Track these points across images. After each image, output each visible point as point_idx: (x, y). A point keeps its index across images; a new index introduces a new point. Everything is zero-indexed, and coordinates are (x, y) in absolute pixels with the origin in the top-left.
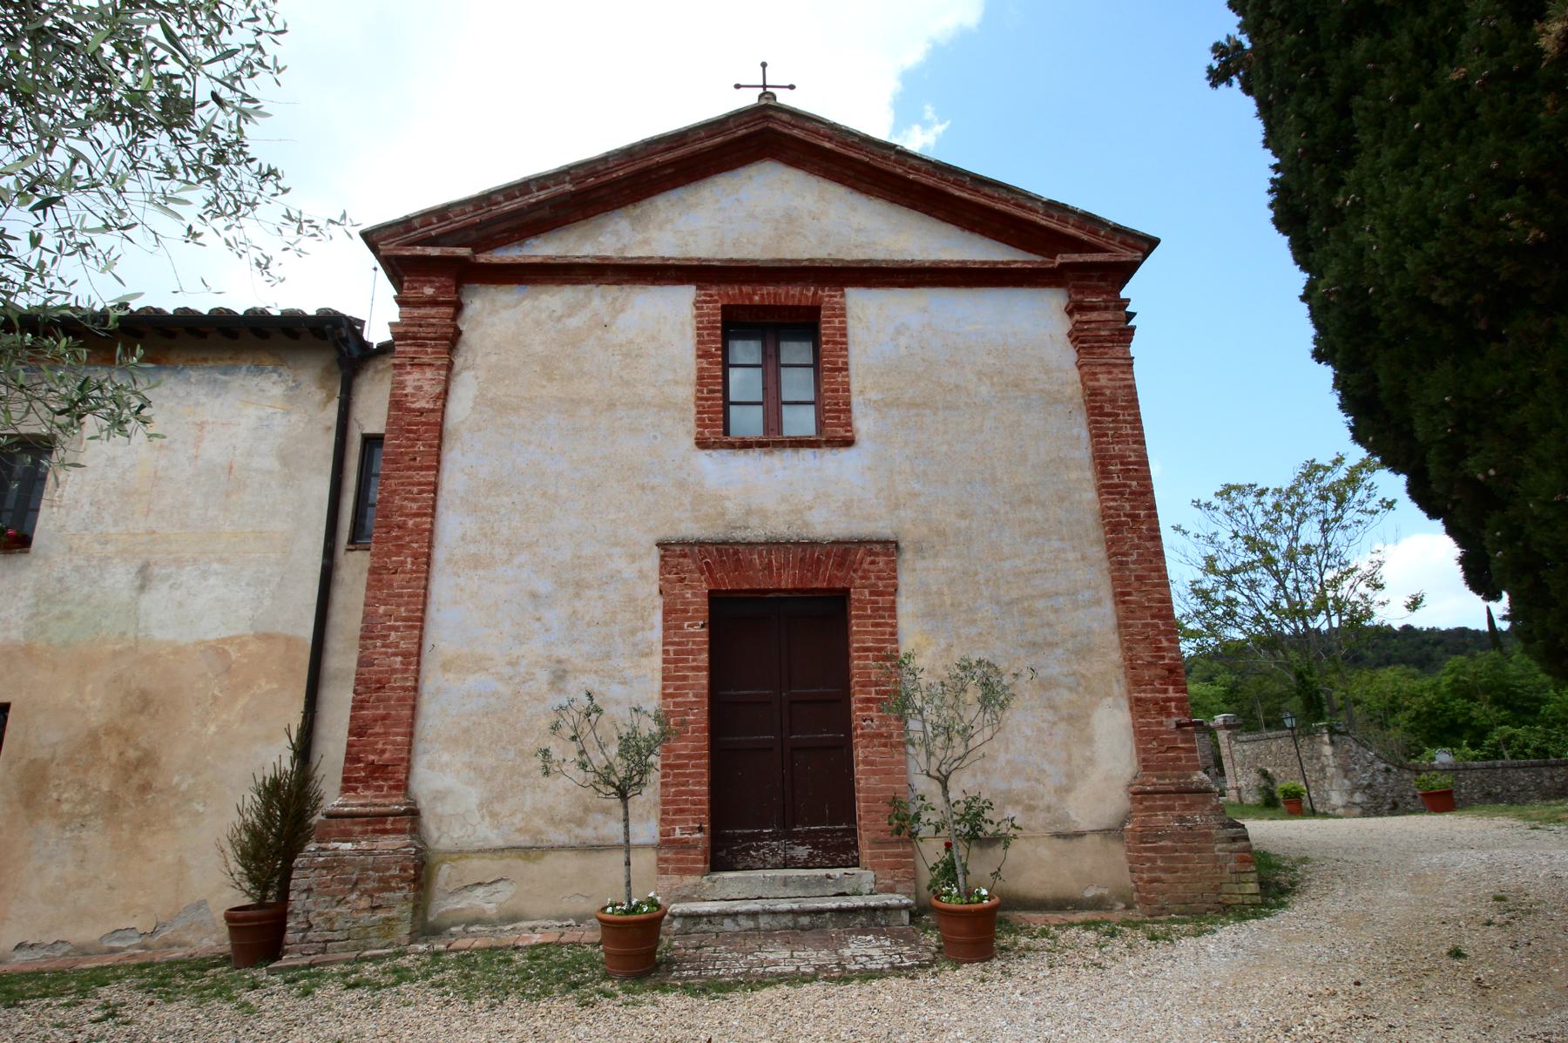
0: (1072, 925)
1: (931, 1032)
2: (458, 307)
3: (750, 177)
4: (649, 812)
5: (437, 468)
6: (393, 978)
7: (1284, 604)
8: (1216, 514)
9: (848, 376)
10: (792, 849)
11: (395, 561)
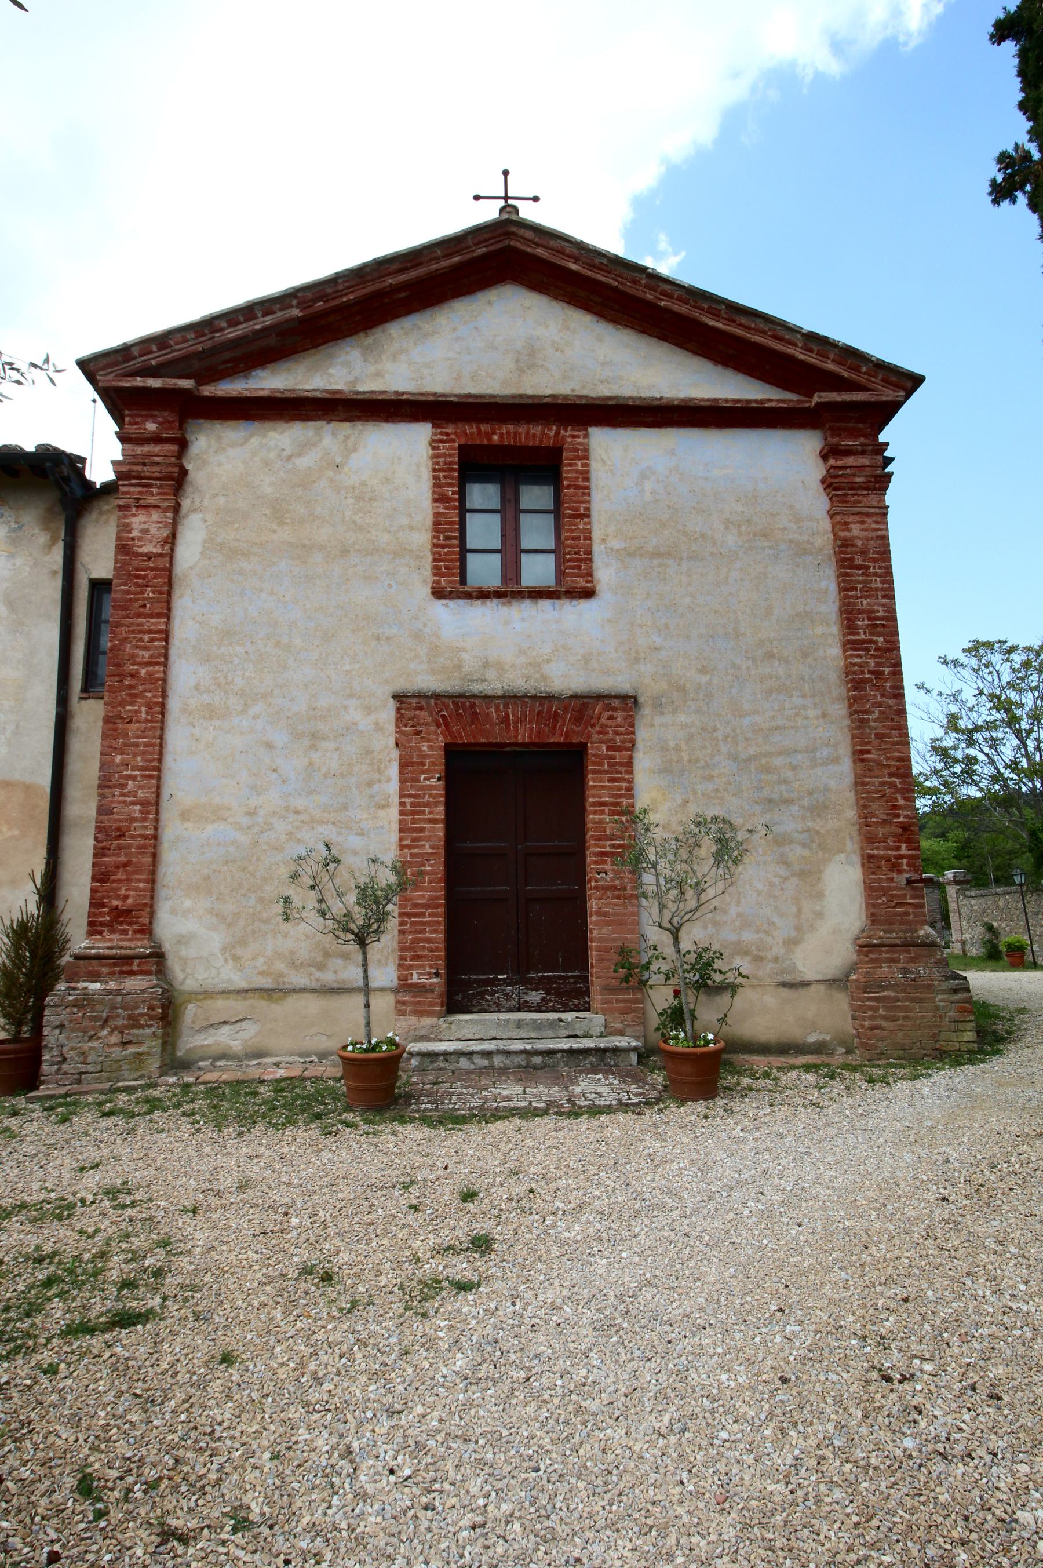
0: (793, 1067)
1: (656, 1163)
2: (183, 445)
3: (490, 303)
4: (387, 958)
5: (167, 615)
6: (145, 1108)
7: (1024, 763)
8: (962, 671)
9: (589, 523)
10: (526, 994)
11: (130, 711)
